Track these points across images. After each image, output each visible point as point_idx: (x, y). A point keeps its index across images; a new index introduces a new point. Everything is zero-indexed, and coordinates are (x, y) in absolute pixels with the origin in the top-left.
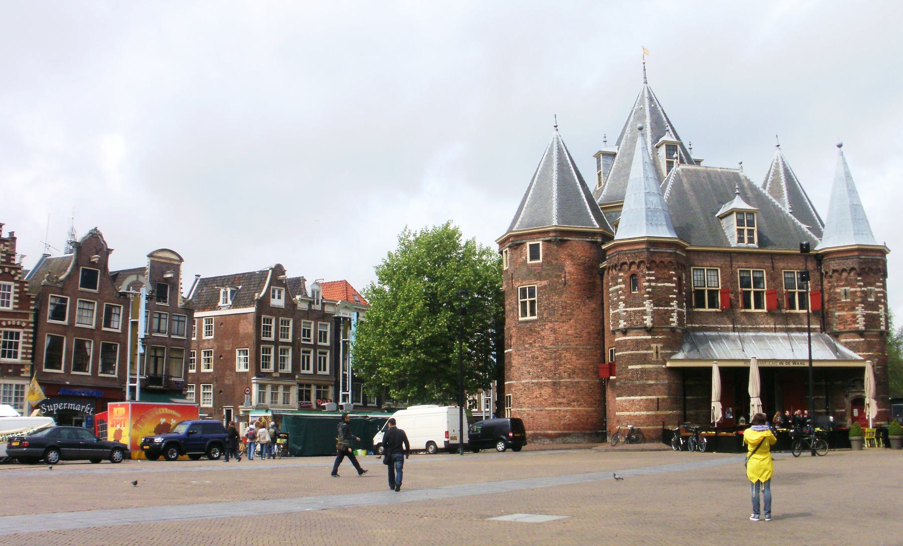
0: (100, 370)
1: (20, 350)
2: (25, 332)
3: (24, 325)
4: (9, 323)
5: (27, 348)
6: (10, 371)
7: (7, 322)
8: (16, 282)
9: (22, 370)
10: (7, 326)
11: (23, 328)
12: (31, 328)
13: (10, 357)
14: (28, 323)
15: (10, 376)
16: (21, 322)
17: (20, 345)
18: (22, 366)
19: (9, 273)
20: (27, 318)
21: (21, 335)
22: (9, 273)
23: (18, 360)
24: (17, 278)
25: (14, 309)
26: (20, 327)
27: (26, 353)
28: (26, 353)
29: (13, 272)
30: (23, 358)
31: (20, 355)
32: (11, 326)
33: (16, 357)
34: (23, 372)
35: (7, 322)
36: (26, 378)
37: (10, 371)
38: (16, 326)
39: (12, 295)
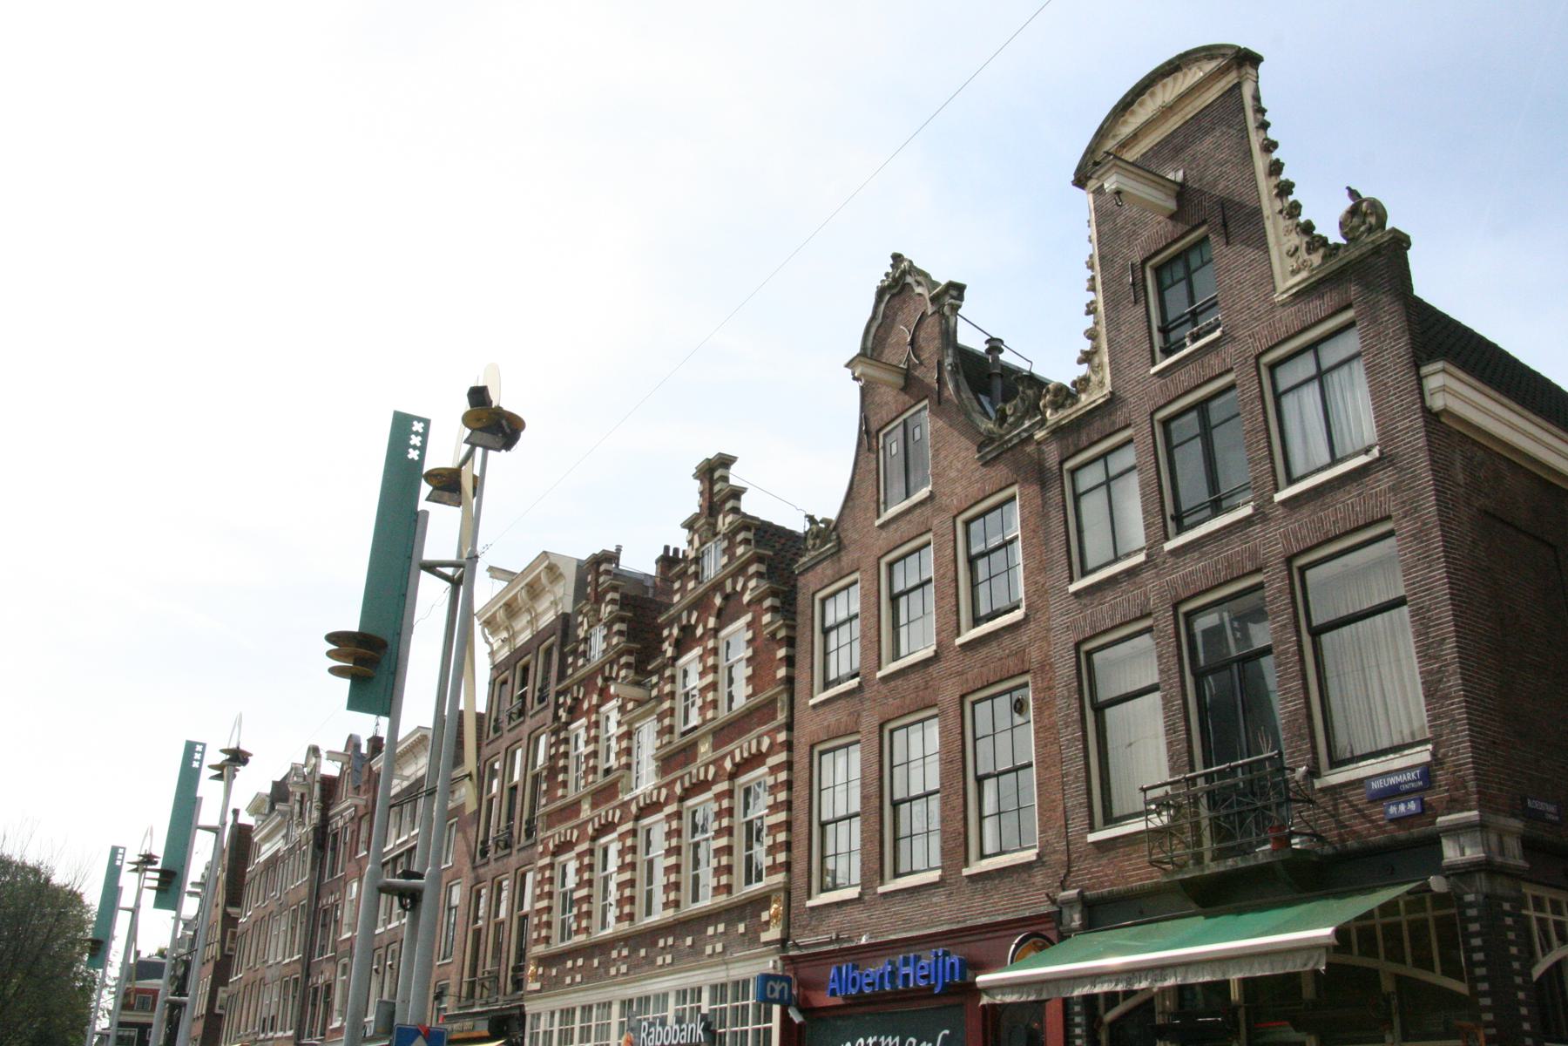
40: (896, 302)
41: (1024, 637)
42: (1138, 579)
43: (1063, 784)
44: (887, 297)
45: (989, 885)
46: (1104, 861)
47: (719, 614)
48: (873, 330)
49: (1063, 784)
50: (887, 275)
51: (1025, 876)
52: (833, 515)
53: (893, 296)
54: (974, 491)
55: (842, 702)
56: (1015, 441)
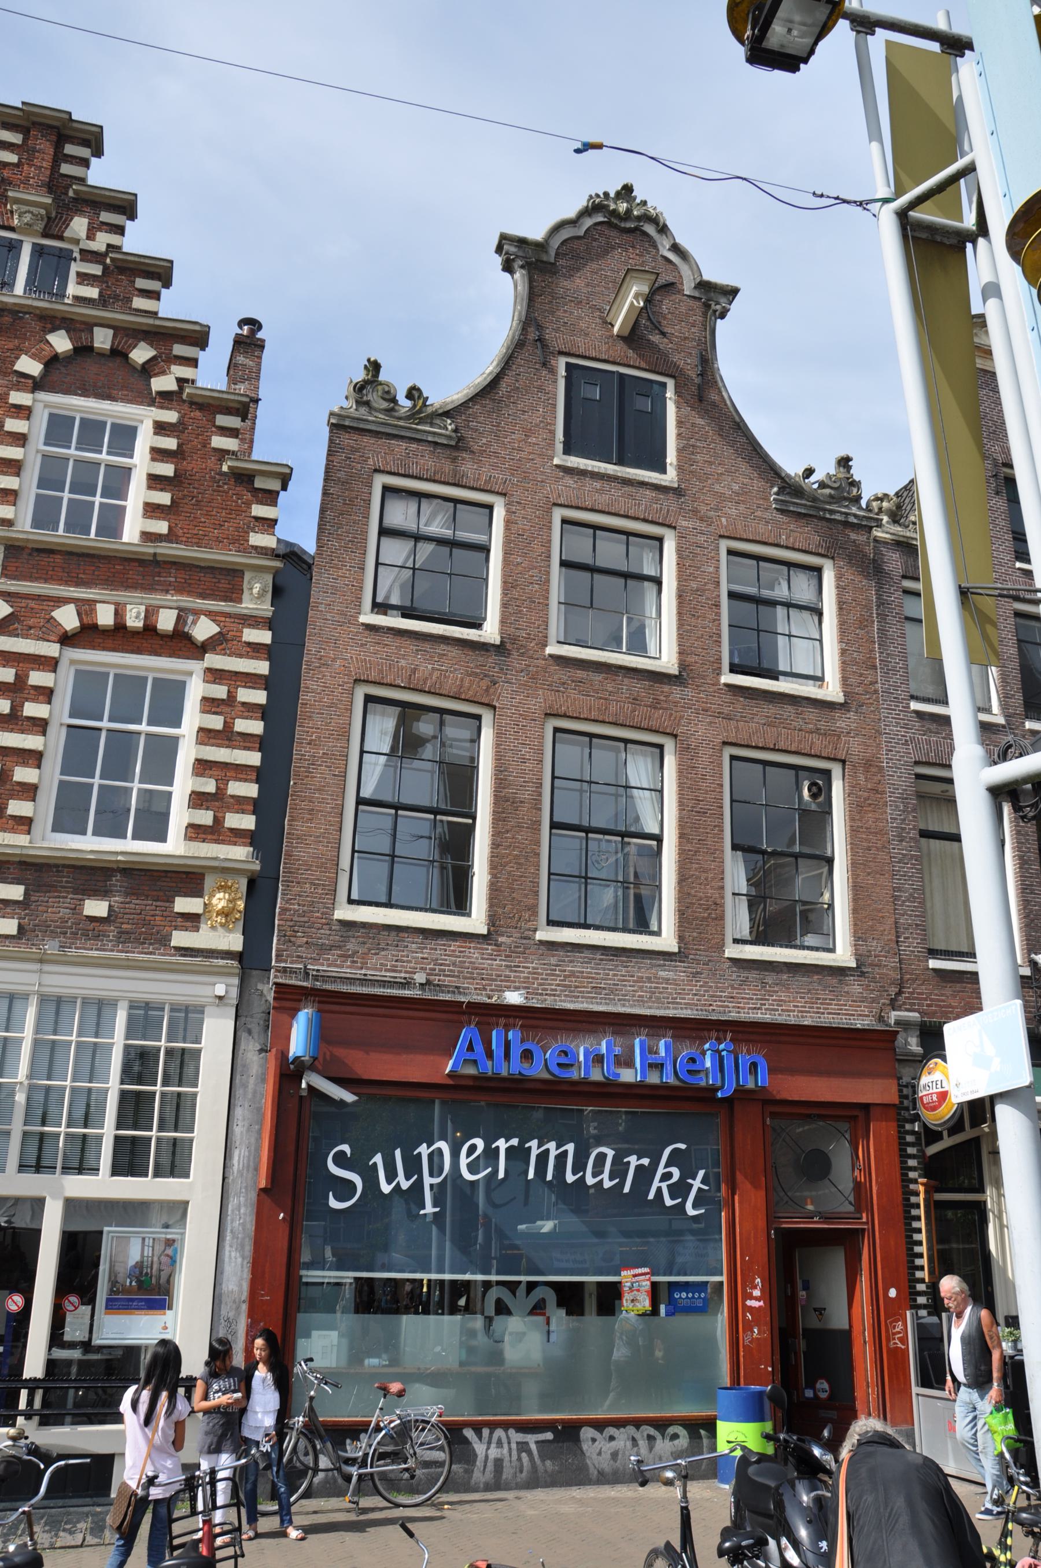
0: (738, 919)
2: (215, 675)
3: (203, 630)
6: (96, 908)
7: (85, 608)
8: (166, 399)
9: (183, 904)
10: (88, 634)
11: (199, 650)
13: (111, 824)
16: (182, 615)
18: (189, 879)
19: (119, 354)
20: (234, 594)
21: (196, 690)
22: (119, 354)
23: (174, 845)
24: (162, 383)
25: (147, 537)
26: (179, 642)
29: (141, 354)
31: (180, 815)
32: (120, 637)
33: (154, 826)
34: (192, 920)
35: (85, 608)
38: (147, 639)
39: (141, 462)
40: (615, 237)
41: (843, 722)
42: (993, 736)
43: (896, 898)
44: (600, 218)
45: (770, 978)
46: (948, 992)
47: (52, 362)
48: (566, 234)
49: (896, 898)
50: (606, 194)
51: (834, 981)
52: (447, 389)
53: (609, 224)
54: (763, 530)
55: (454, 652)
56: (837, 517)
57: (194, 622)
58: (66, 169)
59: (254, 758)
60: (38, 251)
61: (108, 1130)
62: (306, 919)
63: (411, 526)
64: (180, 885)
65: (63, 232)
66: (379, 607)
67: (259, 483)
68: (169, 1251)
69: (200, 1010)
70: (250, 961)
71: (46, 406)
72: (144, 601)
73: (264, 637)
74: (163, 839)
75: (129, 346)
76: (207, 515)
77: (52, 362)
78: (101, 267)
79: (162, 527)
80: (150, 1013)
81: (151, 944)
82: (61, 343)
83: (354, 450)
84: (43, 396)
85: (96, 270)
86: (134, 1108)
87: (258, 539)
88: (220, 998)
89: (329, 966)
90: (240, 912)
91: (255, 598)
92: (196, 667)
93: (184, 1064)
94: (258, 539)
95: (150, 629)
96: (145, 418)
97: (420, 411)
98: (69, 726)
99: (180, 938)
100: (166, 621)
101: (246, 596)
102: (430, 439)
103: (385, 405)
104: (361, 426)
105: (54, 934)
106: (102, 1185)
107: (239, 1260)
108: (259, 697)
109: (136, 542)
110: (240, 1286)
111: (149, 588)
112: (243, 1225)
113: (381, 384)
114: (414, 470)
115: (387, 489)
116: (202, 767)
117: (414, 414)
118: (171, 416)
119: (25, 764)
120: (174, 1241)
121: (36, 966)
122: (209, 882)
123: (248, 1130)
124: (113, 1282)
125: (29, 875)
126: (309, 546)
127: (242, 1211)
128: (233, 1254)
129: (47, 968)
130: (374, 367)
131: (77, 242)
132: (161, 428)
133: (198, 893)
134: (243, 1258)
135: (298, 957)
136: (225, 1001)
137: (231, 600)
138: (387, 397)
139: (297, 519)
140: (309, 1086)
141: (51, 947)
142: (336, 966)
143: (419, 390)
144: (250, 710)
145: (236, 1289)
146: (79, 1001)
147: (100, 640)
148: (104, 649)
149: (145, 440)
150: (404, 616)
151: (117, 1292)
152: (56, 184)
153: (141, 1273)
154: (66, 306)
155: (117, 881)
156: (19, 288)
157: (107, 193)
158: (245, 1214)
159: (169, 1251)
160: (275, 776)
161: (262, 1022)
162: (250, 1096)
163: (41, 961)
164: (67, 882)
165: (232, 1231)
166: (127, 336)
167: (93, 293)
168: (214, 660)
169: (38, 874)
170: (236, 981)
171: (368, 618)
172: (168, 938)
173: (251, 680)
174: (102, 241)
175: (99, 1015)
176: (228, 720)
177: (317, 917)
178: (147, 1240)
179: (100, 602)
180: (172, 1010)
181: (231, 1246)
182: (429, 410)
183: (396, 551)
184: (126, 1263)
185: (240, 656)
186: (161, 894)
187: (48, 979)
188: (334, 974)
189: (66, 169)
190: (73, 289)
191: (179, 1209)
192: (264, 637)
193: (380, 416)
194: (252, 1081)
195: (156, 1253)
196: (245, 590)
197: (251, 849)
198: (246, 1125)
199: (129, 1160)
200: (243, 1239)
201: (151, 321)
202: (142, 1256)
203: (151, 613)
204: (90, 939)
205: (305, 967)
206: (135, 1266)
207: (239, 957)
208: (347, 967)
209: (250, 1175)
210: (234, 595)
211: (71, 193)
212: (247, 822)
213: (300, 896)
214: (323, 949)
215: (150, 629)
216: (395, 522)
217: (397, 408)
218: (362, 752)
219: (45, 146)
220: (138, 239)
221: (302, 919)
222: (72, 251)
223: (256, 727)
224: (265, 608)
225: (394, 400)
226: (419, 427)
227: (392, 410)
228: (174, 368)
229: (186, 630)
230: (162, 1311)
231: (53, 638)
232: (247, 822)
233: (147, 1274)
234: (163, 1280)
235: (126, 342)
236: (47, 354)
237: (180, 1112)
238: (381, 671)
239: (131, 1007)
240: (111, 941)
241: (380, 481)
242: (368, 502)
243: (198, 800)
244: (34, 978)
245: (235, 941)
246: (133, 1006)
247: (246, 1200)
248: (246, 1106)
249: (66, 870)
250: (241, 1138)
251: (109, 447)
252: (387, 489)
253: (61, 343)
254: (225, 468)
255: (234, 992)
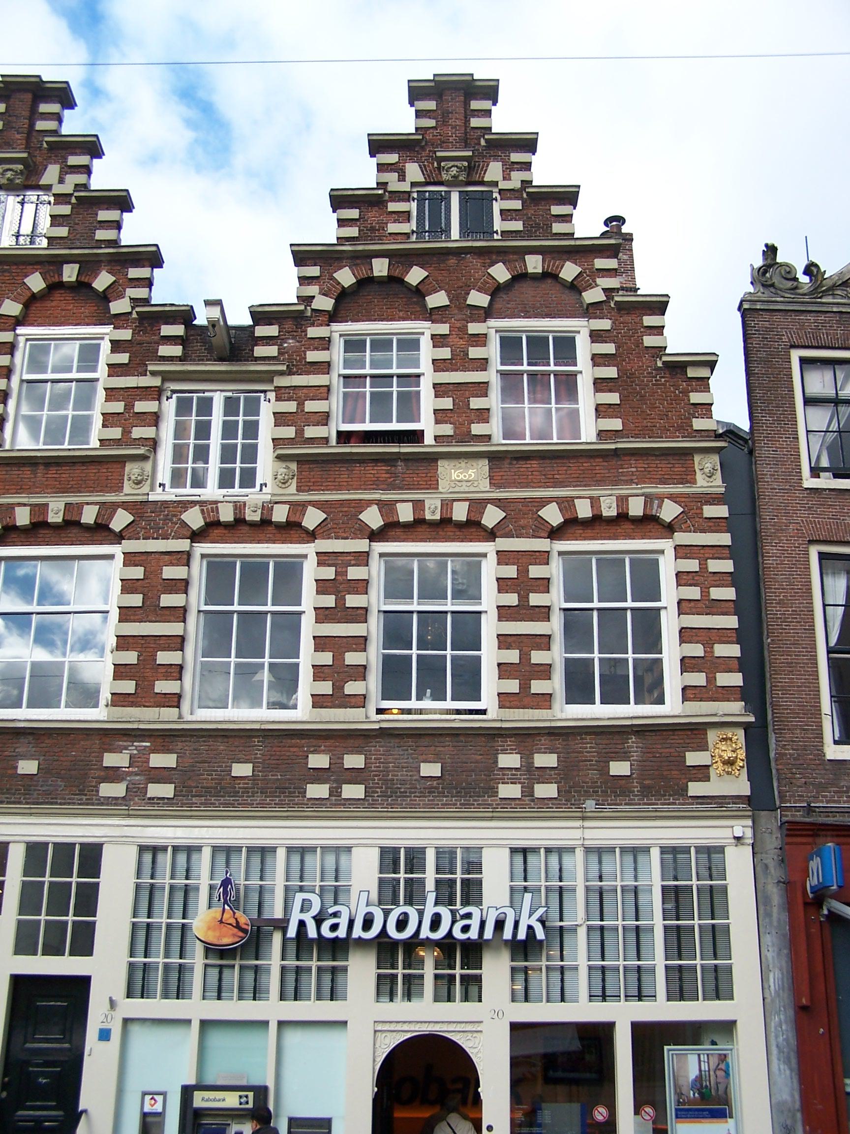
1: (671, 651)
3: (669, 511)
4: (584, 510)
5: (708, 637)
6: (620, 768)
7: (566, 504)
9: (693, 758)
11: (669, 529)
12: (714, 525)
13: (615, 693)
14: (692, 506)
15: (614, 795)
17: (670, 624)
18: (693, 733)
19: (550, 276)
20: (688, 477)
23: (672, 707)
24: (593, 296)
27: (706, 664)
28: (706, 664)
29: (569, 271)
30: (688, 693)
31: (673, 680)
33: (651, 690)
34: (702, 773)
35: (566, 504)
36: (719, 805)
37: (620, 768)
39: (586, 373)
57: (660, 506)
58: (475, 122)
59: (732, 622)
60: (465, 198)
61: (658, 959)
62: (801, 762)
63: (830, 392)
64: (688, 741)
65: (483, 177)
66: (815, 472)
67: (691, 373)
68: (722, 1066)
69: (721, 850)
70: (757, 802)
71: (497, 331)
72: (614, 492)
73: (722, 511)
74: (661, 701)
75: (557, 267)
76: (653, 407)
77: (497, 291)
78: (520, 202)
79: (616, 424)
80: (678, 856)
81: (670, 795)
82: (500, 273)
83: (769, 330)
84: (493, 323)
85: (517, 205)
86: (678, 940)
87: (699, 424)
88: (738, 839)
89: (827, 802)
90: (743, 760)
91: (707, 476)
92: (667, 545)
93: (716, 900)
94: (699, 424)
95: (623, 516)
96: (580, 328)
97: (821, 286)
98: (565, 610)
99: (695, 789)
100: (636, 508)
101: (699, 476)
102: (835, 310)
103: (789, 284)
104: (771, 307)
105: (588, 795)
106: (662, 1009)
107: (788, 1072)
108: (727, 566)
109: (594, 440)
110: (792, 1096)
111: (616, 482)
112: (787, 1040)
113: (781, 265)
114: (824, 339)
115: (803, 361)
116: (686, 635)
117: (816, 289)
118: (605, 324)
119: (539, 648)
120: (725, 1056)
121: (578, 823)
122: (712, 736)
123: (779, 954)
124: (679, 1094)
125: (559, 743)
126: (744, 425)
127: (784, 1027)
128: (782, 1067)
129: (587, 824)
130: (771, 251)
131: (496, 184)
132: (596, 336)
133: (703, 747)
134: (791, 1070)
135: (799, 796)
136: (742, 841)
137: (687, 482)
138: (789, 276)
139: (728, 401)
140: (829, 910)
141: (590, 804)
142: (834, 802)
143: (816, 266)
144: (720, 579)
145: (789, 1098)
146: (617, 850)
147: (581, 531)
148: (585, 539)
149: (584, 348)
150: (836, 476)
151: (684, 1104)
152: (470, 137)
153: (702, 1085)
154: (498, 241)
155: (633, 742)
156: (455, 233)
157: (513, 137)
158: (787, 1030)
159: (722, 1066)
160: (752, 634)
161: (775, 857)
162: (775, 924)
163: (584, 818)
164: (591, 747)
165: (777, 1046)
166: (553, 258)
167: (518, 226)
168: (682, 538)
169: (565, 743)
170: (749, 822)
171: (809, 482)
172: (686, 789)
173: (716, 551)
174: (516, 179)
175: (635, 861)
176: (704, 590)
177: (811, 759)
178: (702, 1056)
179: (577, 498)
180: (697, 852)
181: (779, 1060)
182: (829, 283)
183: (820, 418)
184: (687, 1077)
185: (703, 531)
186: (672, 750)
187: (588, 834)
188: (833, 810)
189: (475, 122)
190: (498, 224)
191: (728, 1027)
192: (722, 511)
193: (787, 295)
194: (775, 910)
195: (712, 1067)
196: (697, 471)
197: (743, 703)
198: (776, 949)
199: (681, 987)
200: (789, 1053)
201: (572, 243)
202: (700, 1070)
203: (622, 501)
204: (619, 796)
205: (809, 805)
206: (695, 1080)
207: (749, 800)
208: (844, 802)
209: (786, 995)
210: (689, 477)
211: (483, 142)
212: (736, 679)
213: (793, 741)
214: (821, 787)
215: (623, 516)
216: (815, 391)
217: (800, 285)
218: (825, 606)
219: (455, 104)
220: (545, 172)
221: (798, 762)
222: (492, 192)
223: (728, 593)
224: (717, 485)
225: (795, 279)
226: (823, 300)
227: (796, 288)
228: (599, 281)
229: (654, 513)
230: (724, 1120)
231: (542, 535)
232: (736, 679)
233: (706, 1086)
234: (721, 1092)
235: (553, 265)
236: (491, 286)
237: (718, 940)
238: (830, 531)
239: (662, 853)
240: (636, 796)
241: (796, 355)
242: (790, 376)
243: (687, 664)
244: (577, 834)
245: (743, 787)
246: (664, 850)
247: (786, 1017)
248: (774, 932)
249: (588, 737)
250: (774, 962)
251: (555, 359)
252: (803, 361)
253: (500, 273)
254: (659, 364)
255: (749, 833)
